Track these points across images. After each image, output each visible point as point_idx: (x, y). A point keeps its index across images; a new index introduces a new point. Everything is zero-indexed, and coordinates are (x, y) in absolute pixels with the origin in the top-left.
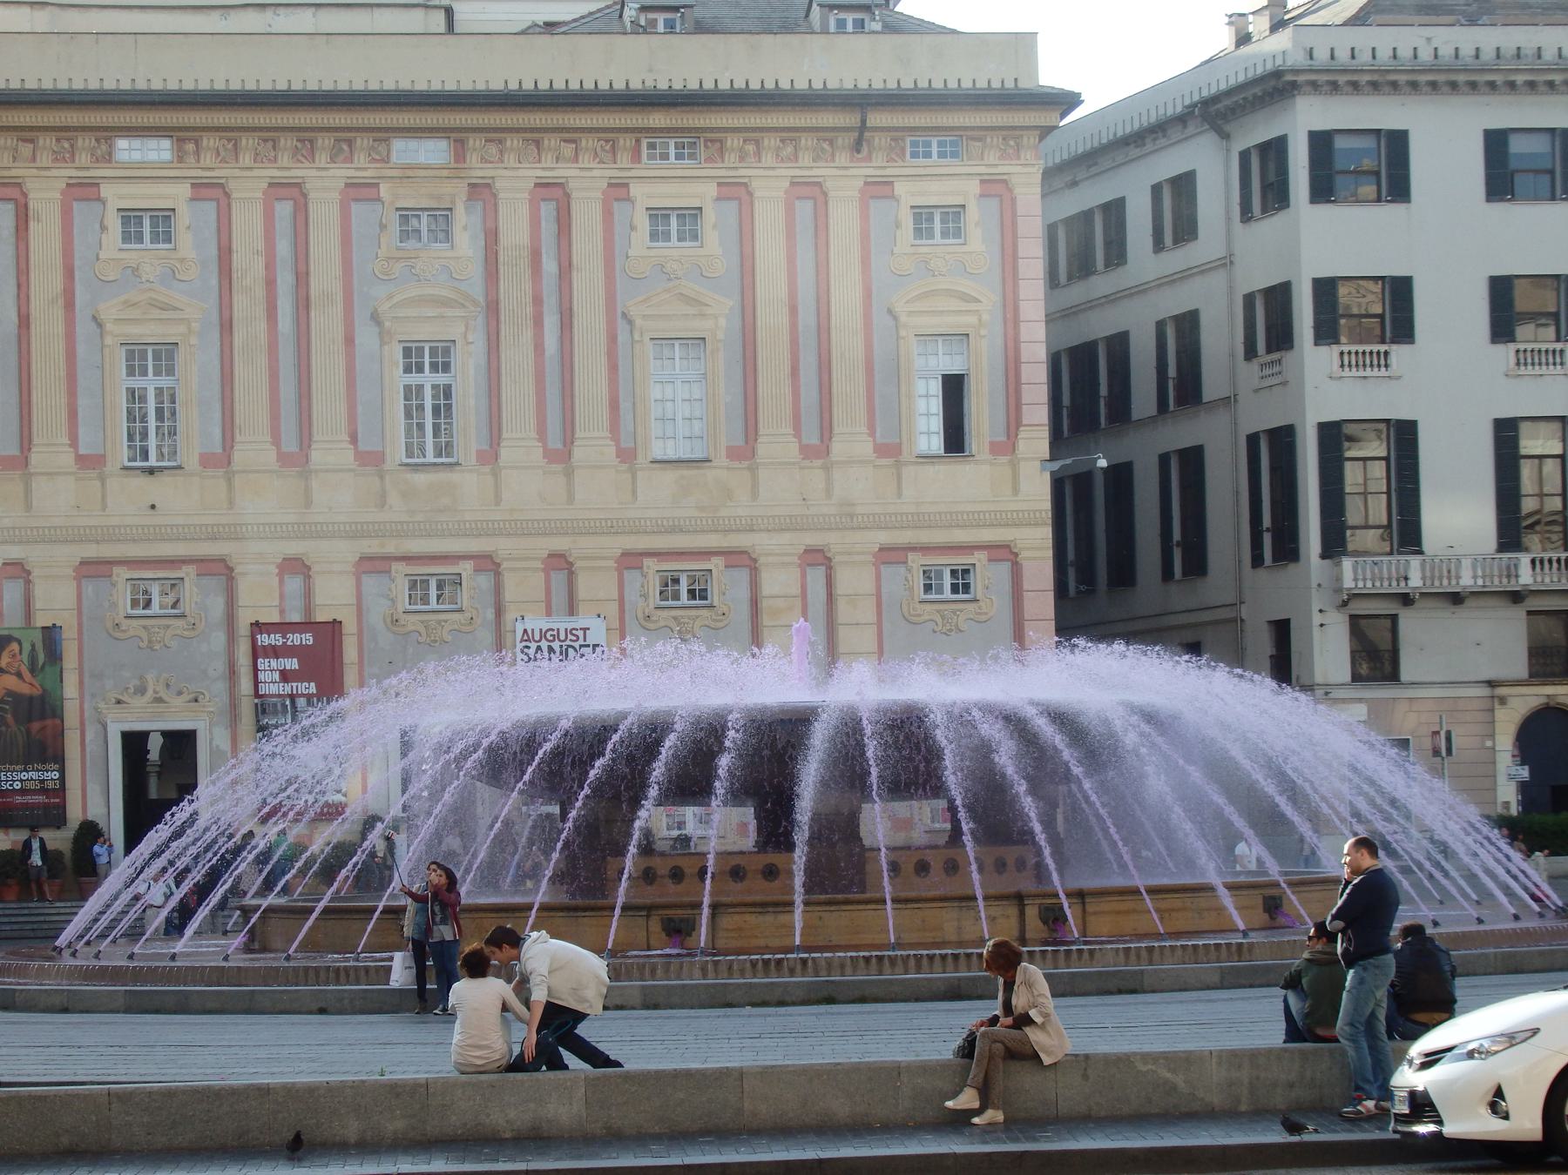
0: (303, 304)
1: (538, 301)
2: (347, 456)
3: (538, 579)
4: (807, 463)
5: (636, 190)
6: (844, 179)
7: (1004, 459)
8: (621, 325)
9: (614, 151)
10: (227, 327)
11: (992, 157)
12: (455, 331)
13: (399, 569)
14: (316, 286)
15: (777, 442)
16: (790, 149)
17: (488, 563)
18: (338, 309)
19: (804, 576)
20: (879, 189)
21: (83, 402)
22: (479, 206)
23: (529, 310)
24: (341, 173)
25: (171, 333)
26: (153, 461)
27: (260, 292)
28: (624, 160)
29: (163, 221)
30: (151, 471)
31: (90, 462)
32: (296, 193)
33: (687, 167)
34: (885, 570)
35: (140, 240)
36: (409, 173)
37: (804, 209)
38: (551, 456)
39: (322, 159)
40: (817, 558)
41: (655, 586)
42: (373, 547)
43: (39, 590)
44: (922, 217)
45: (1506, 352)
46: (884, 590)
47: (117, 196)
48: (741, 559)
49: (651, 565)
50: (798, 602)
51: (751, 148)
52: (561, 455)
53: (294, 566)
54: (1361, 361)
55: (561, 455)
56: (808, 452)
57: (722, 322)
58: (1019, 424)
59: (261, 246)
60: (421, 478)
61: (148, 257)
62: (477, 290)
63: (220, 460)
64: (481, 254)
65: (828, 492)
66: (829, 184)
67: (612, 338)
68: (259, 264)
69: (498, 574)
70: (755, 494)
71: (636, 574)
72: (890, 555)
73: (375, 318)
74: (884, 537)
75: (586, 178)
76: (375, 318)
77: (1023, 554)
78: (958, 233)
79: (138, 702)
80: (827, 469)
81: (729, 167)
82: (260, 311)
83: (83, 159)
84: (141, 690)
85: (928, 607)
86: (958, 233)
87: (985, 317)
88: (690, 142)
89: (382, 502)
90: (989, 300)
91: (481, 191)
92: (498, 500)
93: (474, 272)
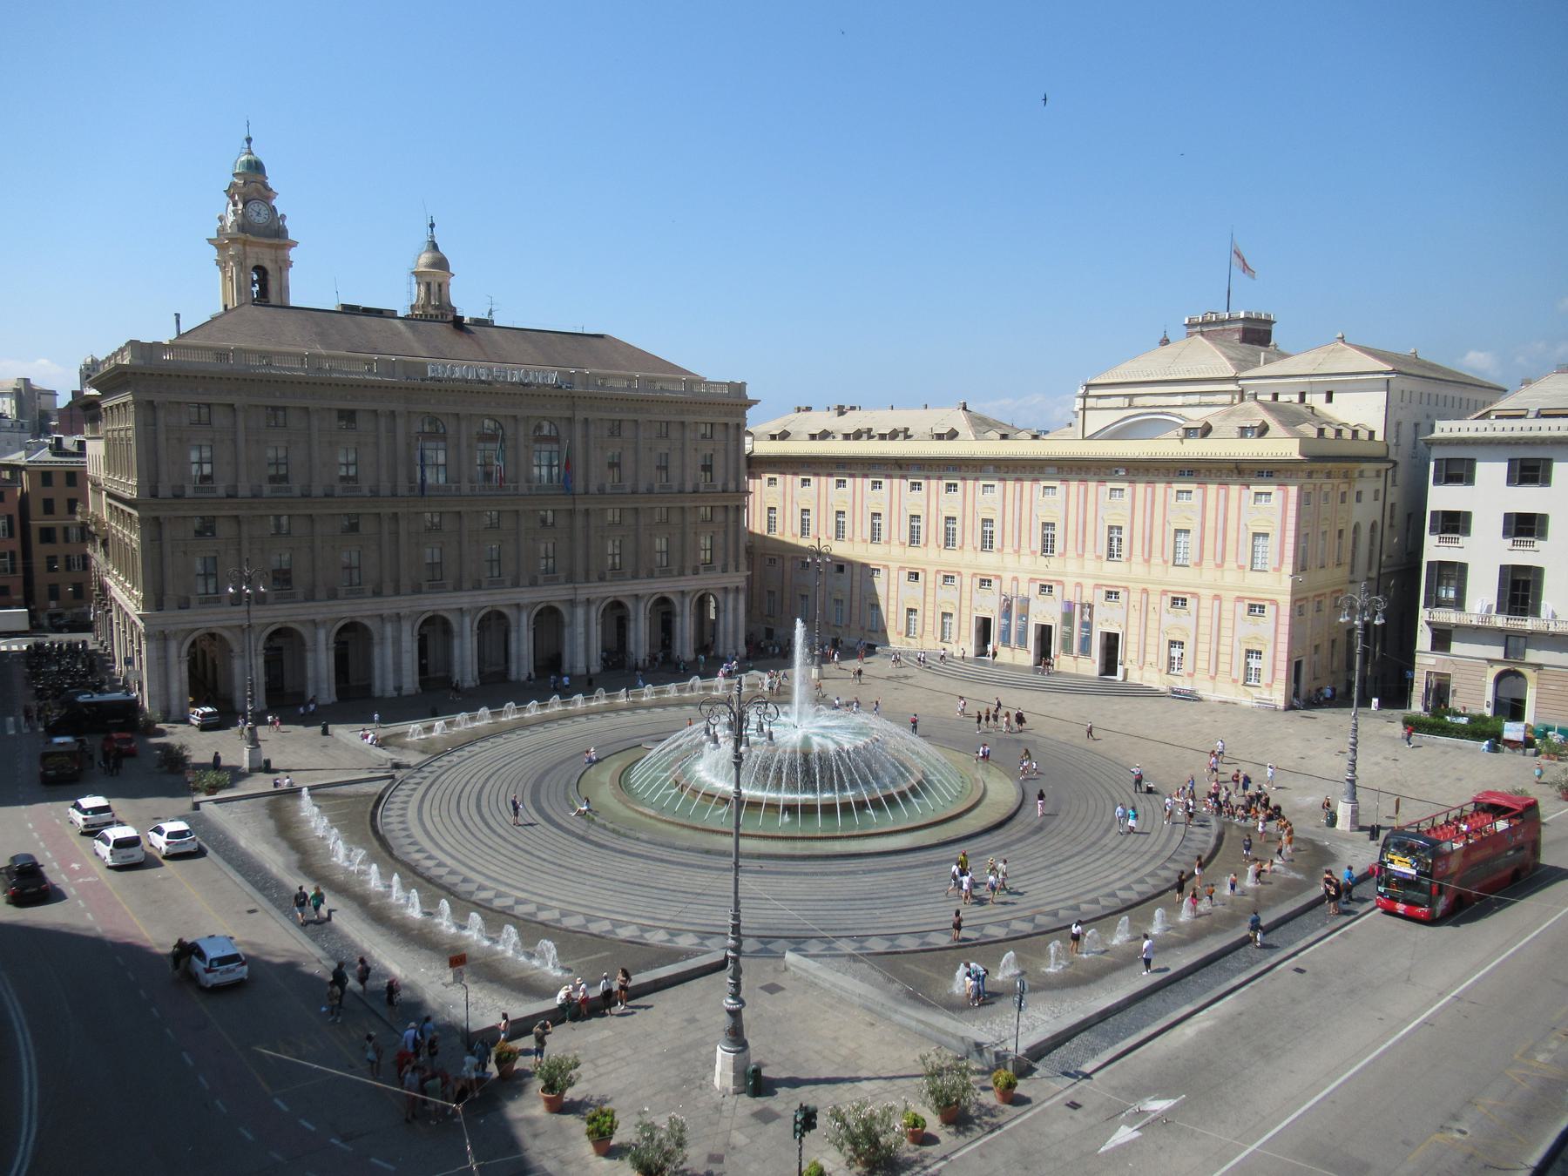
17: (1126, 589)
31: (1034, 553)
45: (1510, 541)
48: (1194, 595)
53: (1079, 585)
54: (1448, 540)
55: (1147, 561)
72: (1240, 599)
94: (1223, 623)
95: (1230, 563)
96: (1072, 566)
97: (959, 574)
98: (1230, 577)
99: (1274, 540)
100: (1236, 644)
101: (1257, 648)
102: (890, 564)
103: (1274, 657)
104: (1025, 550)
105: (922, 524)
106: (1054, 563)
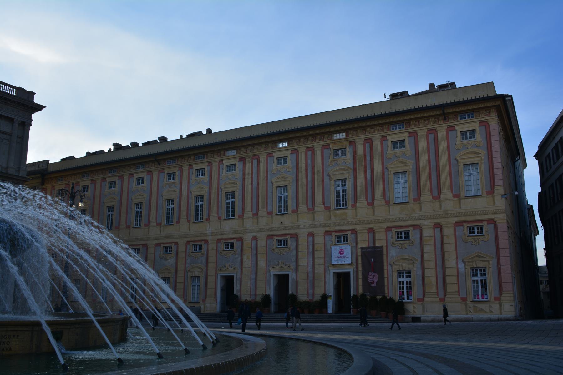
0: (313, 174)
1: (365, 167)
2: (322, 208)
3: (366, 235)
4: (434, 201)
5: (388, 137)
6: (442, 128)
7: (490, 196)
8: (386, 170)
9: (383, 129)
10: (297, 181)
11: (482, 116)
12: (346, 176)
13: (334, 234)
14: (316, 170)
15: (426, 196)
16: (427, 122)
17: (354, 231)
18: (321, 173)
19: (434, 231)
20: (451, 128)
21: (269, 200)
22: (352, 147)
23: (363, 169)
24: (322, 143)
25: (286, 183)
26: (283, 212)
27: (304, 172)
28: (385, 131)
29: (285, 158)
30: (280, 214)
31: (270, 213)
32: (312, 149)
33: (402, 130)
34: (457, 228)
35: (281, 164)
36: (336, 141)
37: (431, 136)
38: (368, 204)
39: (317, 141)
40: (438, 226)
41: (395, 236)
42: (328, 229)
43: (259, 242)
44: (464, 134)
46: (457, 234)
47: (276, 155)
48: (418, 227)
49: (394, 230)
50: (433, 238)
51: (417, 123)
52: (371, 204)
53: (311, 235)
55: (371, 204)
56: (434, 198)
57: (411, 167)
58: (494, 185)
59: (304, 162)
60: (339, 212)
61: (282, 167)
62: (351, 166)
63: (295, 211)
64: (352, 158)
65: (440, 208)
66: (438, 129)
67: (383, 174)
68: (304, 166)
69: (356, 234)
70: (421, 210)
71: (390, 232)
72: (458, 224)
73: (329, 175)
74: (456, 219)
75: (376, 136)
76: (329, 175)
77: (498, 222)
78: (474, 137)
79: (277, 267)
80: (440, 202)
81: (412, 128)
82: (304, 176)
83: (270, 148)
84: (278, 265)
85: (470, 238)
86: (474, 137)
87: (483, 158)
88: (401, 122)
89: (330, 218)
90: (484, 153)
91: (352, 143)
92: (356, 216)
93: (351, 162)
94: (447, 247)
95: (446, 194)
96: (304, 220)
97: (206, 241)
98: (449, 205)
99: (484, 167)
100: (461, 266)
101: (481, 264)
102: (149, 242)
103: (499, 269)
104: (263, 212)
105: (176, 206)
106: (288, 220)
